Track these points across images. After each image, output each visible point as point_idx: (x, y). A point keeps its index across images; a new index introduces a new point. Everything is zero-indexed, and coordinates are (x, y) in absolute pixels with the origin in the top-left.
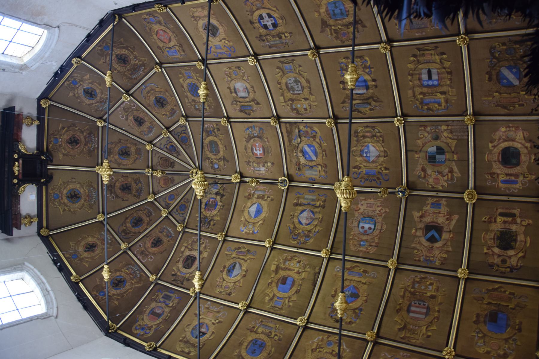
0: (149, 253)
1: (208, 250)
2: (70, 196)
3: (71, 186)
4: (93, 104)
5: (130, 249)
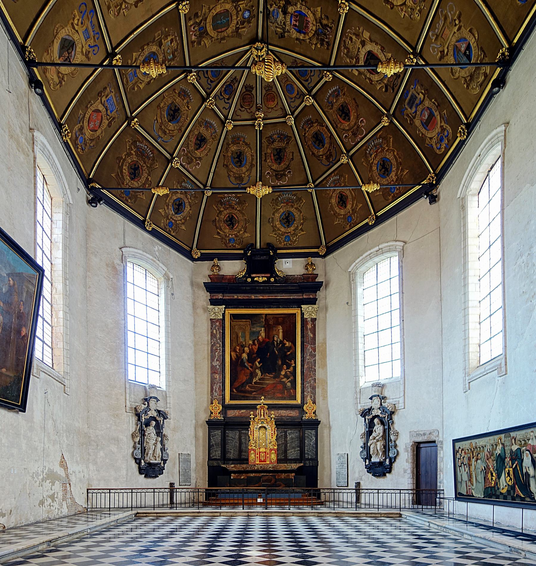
0: (355, 124)
1: (361, 29)
2: (287, 224)
3: (278, 224)
4: (189, 202)
5: (348, 151)
